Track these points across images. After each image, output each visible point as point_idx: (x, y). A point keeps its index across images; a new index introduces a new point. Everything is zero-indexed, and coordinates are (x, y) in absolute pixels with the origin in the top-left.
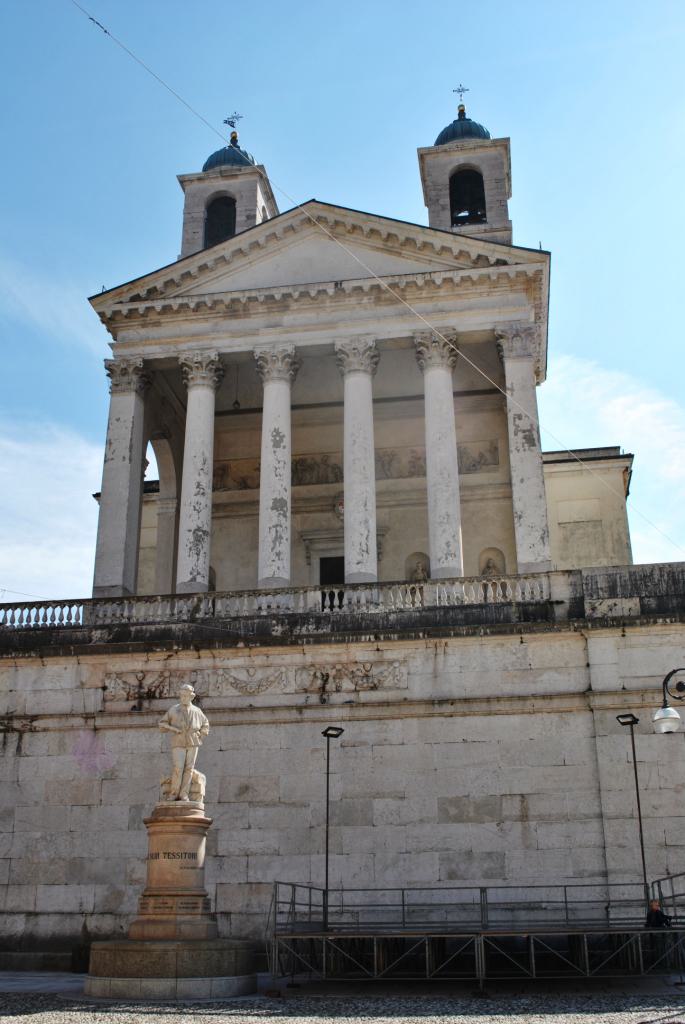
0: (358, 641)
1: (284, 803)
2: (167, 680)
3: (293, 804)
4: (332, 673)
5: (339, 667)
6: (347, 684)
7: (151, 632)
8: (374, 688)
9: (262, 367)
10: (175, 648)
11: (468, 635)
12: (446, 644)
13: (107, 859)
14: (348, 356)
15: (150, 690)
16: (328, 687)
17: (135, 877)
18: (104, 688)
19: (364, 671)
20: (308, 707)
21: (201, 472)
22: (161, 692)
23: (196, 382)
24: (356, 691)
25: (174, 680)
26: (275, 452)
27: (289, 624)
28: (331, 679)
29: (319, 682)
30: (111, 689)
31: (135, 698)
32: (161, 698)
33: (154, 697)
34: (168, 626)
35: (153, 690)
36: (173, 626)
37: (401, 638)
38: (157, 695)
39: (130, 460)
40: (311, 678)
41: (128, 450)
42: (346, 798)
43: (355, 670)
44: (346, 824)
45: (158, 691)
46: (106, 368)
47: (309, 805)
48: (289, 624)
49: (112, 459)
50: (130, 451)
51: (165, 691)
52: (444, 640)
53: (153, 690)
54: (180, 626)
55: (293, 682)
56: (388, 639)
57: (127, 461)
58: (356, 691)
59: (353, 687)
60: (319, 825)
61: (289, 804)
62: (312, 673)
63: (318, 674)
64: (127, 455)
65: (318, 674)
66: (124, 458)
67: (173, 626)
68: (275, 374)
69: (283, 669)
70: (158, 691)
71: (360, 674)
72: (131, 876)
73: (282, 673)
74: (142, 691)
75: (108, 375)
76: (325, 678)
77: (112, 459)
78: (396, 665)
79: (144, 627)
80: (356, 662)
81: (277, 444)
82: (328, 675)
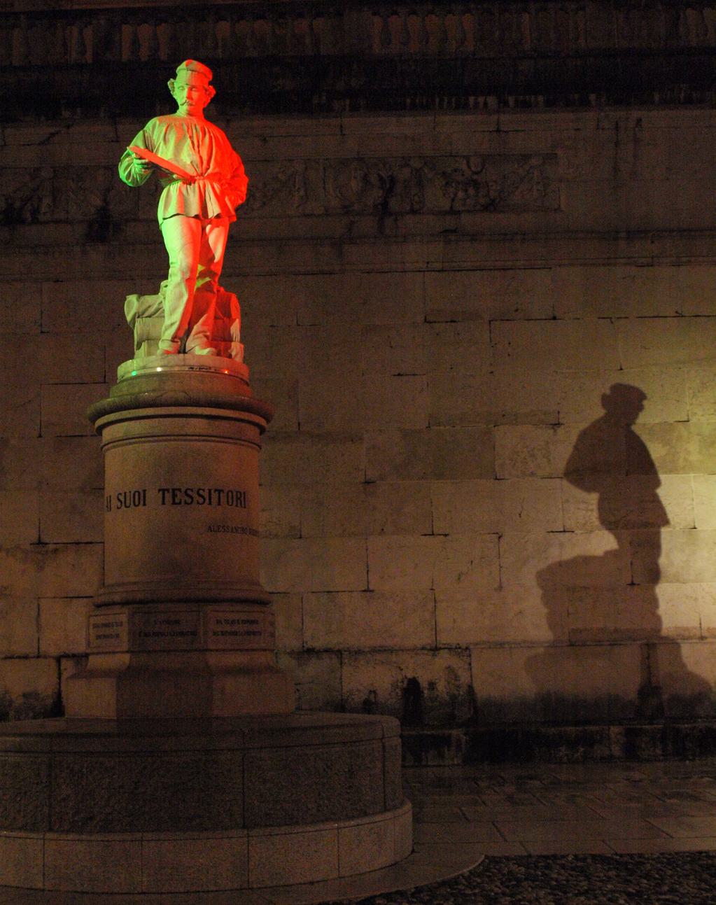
0: (461, 107)
5: (416, 164)
6: (436, 197)
8: (490, 206)
10: (66, 114)
11: (689, 101)
12: (639, 120)
22: (35, 212)
24: (452, 212)
29: (376, 194)
32: (35, 221)
37: (550, 104)
47: (361, 439)
52: (636, 114)
53: (17, 204)
56: (525, 106)
58: (452, 212)
59: (445, 204)
63: (373, 179)
65: (373, 179)
71: (461, 179)
76: (389, 185)
78: (534, 161)
82: (393, 180)
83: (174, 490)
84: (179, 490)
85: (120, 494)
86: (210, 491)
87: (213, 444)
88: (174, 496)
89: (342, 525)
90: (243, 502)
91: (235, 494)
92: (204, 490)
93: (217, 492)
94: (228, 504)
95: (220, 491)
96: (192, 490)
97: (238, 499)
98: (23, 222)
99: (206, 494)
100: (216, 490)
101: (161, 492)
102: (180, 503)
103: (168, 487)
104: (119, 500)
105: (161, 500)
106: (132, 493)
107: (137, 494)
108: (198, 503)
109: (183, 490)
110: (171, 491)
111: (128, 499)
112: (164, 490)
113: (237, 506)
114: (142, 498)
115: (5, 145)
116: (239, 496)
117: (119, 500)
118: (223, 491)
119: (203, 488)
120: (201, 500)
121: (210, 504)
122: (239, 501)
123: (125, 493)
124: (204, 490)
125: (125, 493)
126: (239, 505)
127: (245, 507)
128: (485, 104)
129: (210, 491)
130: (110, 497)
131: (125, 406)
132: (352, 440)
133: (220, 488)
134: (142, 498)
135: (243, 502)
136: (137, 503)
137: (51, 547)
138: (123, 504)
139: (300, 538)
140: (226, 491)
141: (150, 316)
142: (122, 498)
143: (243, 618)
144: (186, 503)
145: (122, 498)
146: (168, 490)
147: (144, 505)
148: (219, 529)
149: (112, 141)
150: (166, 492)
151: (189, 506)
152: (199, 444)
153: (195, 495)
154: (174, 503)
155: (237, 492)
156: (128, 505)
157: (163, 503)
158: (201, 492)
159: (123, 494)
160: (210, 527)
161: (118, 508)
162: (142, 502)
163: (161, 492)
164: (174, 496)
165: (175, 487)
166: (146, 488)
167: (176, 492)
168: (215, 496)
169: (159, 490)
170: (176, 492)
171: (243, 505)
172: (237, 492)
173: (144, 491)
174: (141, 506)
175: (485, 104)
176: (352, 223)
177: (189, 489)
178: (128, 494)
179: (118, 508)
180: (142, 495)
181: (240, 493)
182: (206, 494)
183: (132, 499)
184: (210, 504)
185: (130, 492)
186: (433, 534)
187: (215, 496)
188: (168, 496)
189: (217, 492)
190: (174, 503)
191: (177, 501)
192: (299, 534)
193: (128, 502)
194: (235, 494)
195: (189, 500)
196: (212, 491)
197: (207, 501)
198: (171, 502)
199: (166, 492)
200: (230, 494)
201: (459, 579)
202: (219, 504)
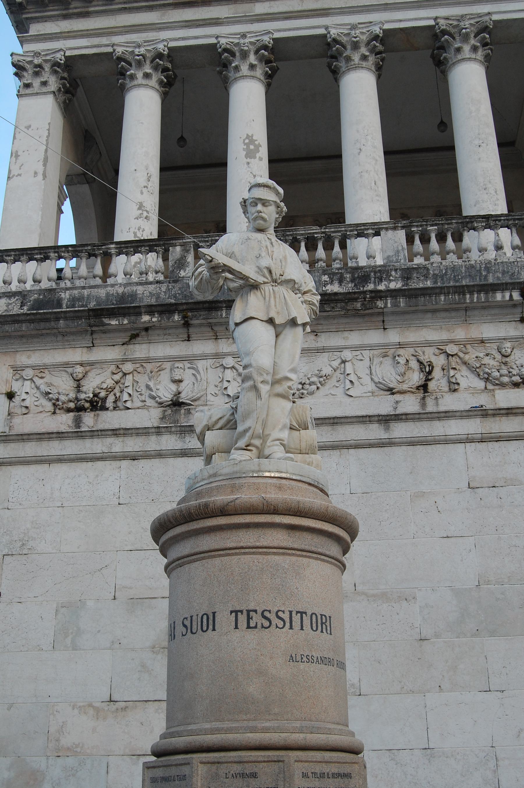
1: (364, 593)
2: (129, 378)
3: (384, 597)
4: (439, 361)
7: (98, 299)
9: (225, 65)
13: (10, 706)
14: (344, 47)
15: (95, 395)
16: (432, 385)
17: (67, 741)
18: (10, 396)
19: (498, 357)
20: (398, 418)
21: (145, 190)
23: (135, 82)
25: (143, 379)
26: (248, 163)
27: (352, 281)
28: (437, 373)
30: (24, 396)
31: (69, 410)
33: (104, 408)
34: (128, 289)
35: (103, 394)
36: (140, 289)
38: (109, 403)
39: (45, 176)
40: (402, 369)
41: (41, 163)
42: (488, 583)
43: (481, 355)
44: (493, 634)
45: (111, 399)
46: (14, 65)
48: (352, 280)
49: (19, 175)
50: (45, 165)
51: (126, 397)
53: (103, 394)
54: (151, 288)
55: (366, 379)
57: (40, 177)
60: (437, 636)
61: (373, 596)
62: (402, 361)
64: (40, 168)
65: (414, 364)
66: (36, 173)
67: (140, 289)
68: (245, 69)
69: (347, 354)
70: (111, 399)
72: (58, 740)
73: (344, 362)
74: (82, 396)
75: (16, 74)
77: (19, 175)
79: (86, 292)
80: (482, 342)
81: (250, 154)
82: (431, 365)
83: (248, 611)
84: (255, 611)
85: (186, 618)
86: (291, 612)
87: (294, 559)
88: (249, 618)
89: (400, 682)
90: (329, 628)
91: (319, 617)
92: (283, 612)
93: (299, 614)
94: (312, 628)
95: (302, 613)
96: (270, 611)
97: (322, 623)
98: (107, 409)
99: (286, 616)
100: (297, 612)
101: (233, 614)
102: (256, 627)
103: (242, 608)
104: (185, 626)
105: (233, 624)
106: (200, 616)
107: (205, 617)
108: (277, 627)
109: (259, 612)
110: (245, 613)
111: (194, 623)
112: (236, 612)
113: (322, 632)
114: (211, 622)
115: (93, 346)
116: (324, 621)
117: (185, 626)
118: (305, 613)
119: (283, 609)
120: (280, 624)
121: (291, 628)
122: (324, 626)
123: (192, 617)
124: (283, 612)
125: (192, 617)
126: (324, 631)
127: (331, 634)
128: (511, 296)
129: (291, 612)
130: (174, 622)
131: (190, 514)
132: (406, 599)
133: (302, 611)
134: (211, 622)
135: (329, 628)
136: (205, 628)
137: (123, 704)
138: (189, 630)
139: (360, 695)
140: (309, 614)
141: (221, 429)
142: (187, 623)
143: (333, 771)
144: (263, 627)
145: (187, 623)
146: (241, 612)
147: (214, 629)
148: (302, 658)
149: (185, 340)
150: (239, 613)
151: (266, 630)
152: (276, 557)
153: (272, 617)
154: (249, 627)
155: (322, 615)
156: (194, 631)
157: (236, 627)
158: (280, 614)
159: (189, 619)
160: (291, 656)
161: (183, 635)
162: (211, 627)
163: (233, 614)
164: (249, 618)
165: (251, 607)
166: (216, 610)
167: (251, 613)
168: (296, 618)
169: (231, 612)
170: (251, 613)
171: (329, 633)
172: (322, 615)
173: (214, 613)
174: (210, 630)
175: (511, 296)
176: (397, 402)
177: (266, 610)
178: (194, 618)
179: (183, 635)
180: (211, 618)
181: (325, 616)
182: (286, 616)
183: (199, 624)
184: (291, 628)
185: (197, 615)
186: (490, 691)
187: (296, 618)
188: (242, 619)
189: (299, 614)
190: (249, 627)
191: (252, 624)
192: (358, 691)
193: (194, 627)
194: (319, 617)
195: (266, 624)
196: (294, 614)
197: (288, 625)
198: (245, 625)
199: (239, 613)
200: (314, 616)
201: (519, 735)
202: (302, 629)
